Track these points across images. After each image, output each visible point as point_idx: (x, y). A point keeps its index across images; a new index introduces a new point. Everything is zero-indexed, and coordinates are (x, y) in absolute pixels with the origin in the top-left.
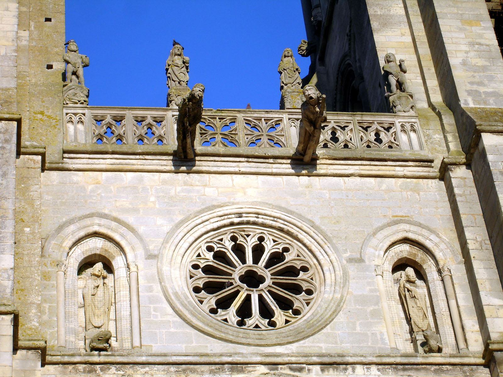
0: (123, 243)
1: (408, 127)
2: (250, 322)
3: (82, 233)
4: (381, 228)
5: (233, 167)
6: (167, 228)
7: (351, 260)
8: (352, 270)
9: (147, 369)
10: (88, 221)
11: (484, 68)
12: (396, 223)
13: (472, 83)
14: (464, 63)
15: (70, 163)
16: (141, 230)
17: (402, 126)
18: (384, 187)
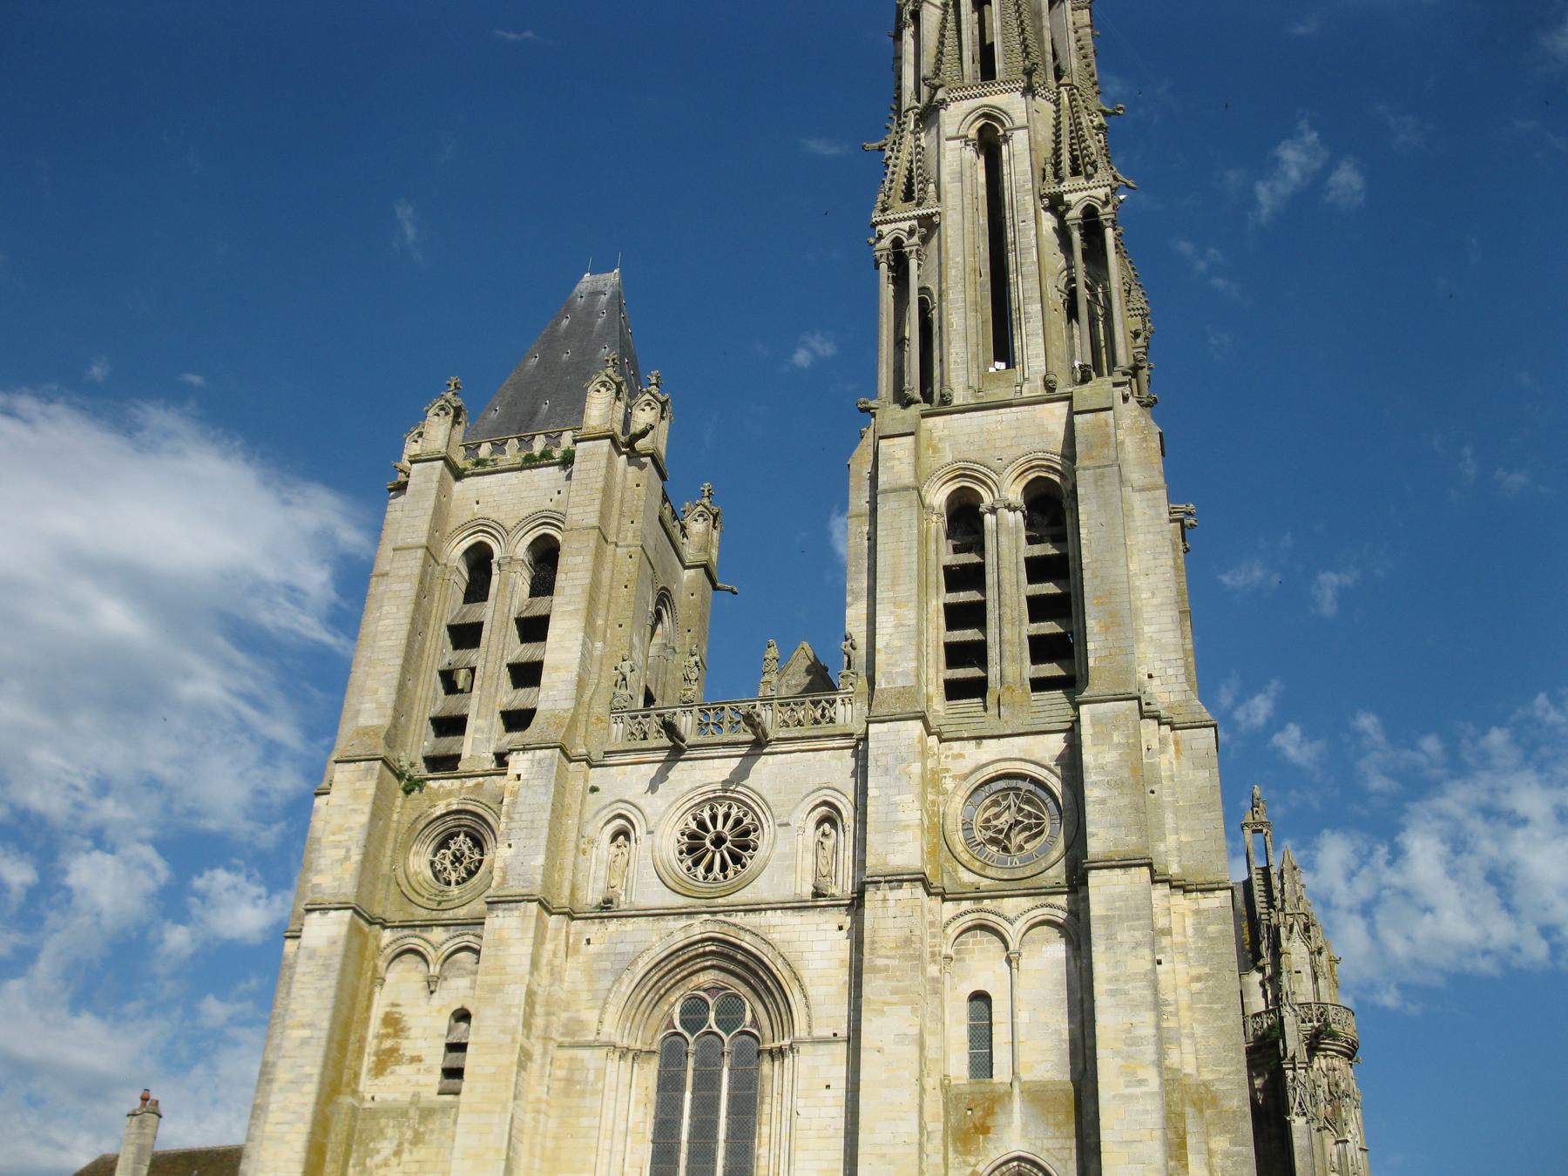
0: (635, 821)
1: (847, 701)
2: (711, 876)
3: (611, 815)
4: (808, 795)
5: (713, 753)
6: (663, 808)
7: (780, 825)
8: (780, 831)
9: (635, 919)
10: (615, 806)
11: (901, 649)
12: (820, 789)
13: (888, 665)
14: (887, 646)
15: (609, 761)
16: (647, 811)
17: (843, 701)
18: (818, 758)
